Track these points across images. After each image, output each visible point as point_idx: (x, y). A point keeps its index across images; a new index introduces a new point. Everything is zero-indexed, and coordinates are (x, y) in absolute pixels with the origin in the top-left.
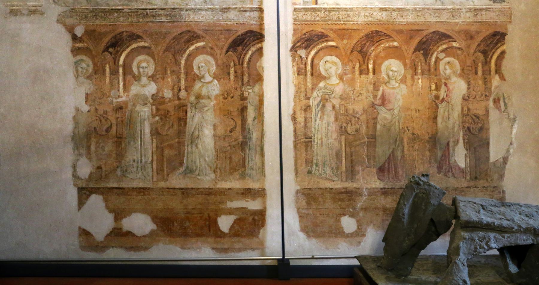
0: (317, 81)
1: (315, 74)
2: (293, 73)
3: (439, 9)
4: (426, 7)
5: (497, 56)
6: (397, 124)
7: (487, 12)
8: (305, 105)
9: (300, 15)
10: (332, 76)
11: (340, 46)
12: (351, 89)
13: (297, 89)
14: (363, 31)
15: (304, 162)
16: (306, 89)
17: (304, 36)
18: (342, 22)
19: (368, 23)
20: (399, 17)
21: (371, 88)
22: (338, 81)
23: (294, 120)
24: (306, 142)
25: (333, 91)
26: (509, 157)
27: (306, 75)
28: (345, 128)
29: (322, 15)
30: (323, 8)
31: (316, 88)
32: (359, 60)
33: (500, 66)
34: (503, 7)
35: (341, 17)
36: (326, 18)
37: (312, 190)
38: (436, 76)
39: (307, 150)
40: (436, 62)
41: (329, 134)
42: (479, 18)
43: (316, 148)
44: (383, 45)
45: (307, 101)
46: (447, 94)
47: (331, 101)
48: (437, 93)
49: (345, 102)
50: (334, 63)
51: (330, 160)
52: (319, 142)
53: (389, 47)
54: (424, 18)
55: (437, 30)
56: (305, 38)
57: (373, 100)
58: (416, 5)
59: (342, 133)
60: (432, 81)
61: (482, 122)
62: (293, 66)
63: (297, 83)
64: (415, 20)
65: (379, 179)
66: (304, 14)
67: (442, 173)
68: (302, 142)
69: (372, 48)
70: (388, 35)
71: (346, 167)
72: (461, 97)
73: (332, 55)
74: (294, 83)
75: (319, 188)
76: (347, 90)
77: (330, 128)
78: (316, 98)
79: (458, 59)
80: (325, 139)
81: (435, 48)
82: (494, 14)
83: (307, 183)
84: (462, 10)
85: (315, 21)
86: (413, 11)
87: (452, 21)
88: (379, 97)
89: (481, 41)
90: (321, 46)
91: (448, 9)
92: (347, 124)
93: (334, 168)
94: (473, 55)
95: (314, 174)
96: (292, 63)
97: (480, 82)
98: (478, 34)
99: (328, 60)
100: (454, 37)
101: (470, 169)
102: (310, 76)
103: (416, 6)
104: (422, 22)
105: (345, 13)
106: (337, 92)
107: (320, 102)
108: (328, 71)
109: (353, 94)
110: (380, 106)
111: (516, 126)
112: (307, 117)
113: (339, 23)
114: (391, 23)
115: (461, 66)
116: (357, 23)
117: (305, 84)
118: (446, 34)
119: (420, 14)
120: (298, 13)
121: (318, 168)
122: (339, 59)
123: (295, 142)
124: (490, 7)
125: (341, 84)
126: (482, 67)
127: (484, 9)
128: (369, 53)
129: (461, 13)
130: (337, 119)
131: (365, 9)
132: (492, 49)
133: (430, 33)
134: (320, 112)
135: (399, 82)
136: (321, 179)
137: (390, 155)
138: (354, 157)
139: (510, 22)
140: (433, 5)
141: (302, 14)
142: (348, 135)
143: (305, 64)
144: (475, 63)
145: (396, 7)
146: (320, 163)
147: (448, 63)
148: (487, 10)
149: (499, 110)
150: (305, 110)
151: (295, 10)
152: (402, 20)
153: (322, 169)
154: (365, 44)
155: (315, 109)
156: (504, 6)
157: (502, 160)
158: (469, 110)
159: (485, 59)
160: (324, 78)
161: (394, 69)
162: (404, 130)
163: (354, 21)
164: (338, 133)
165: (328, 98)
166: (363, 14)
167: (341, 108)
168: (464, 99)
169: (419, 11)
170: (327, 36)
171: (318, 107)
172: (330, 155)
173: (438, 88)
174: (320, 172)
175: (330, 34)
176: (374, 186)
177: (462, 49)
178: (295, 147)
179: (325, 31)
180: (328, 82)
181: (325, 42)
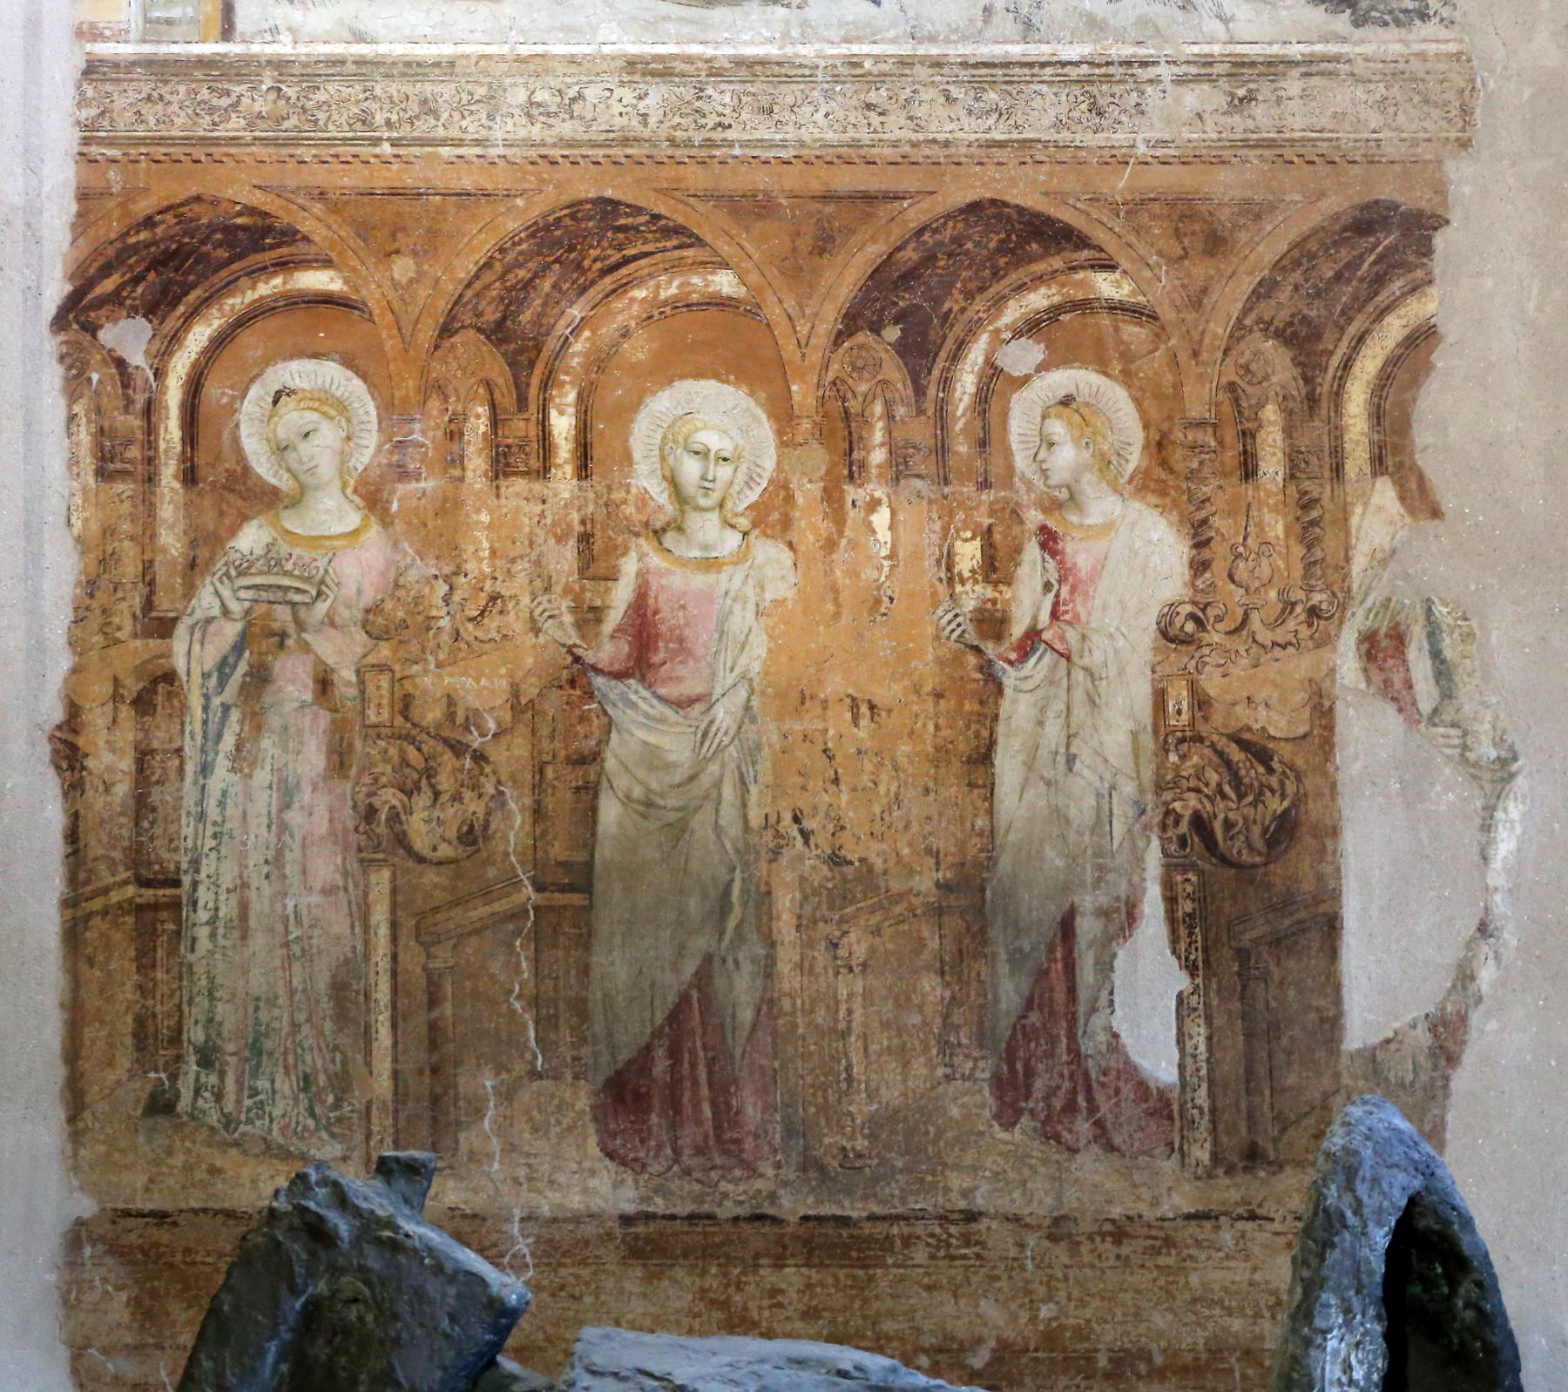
0: (221, 513)
1: (209, 476)
2: (69, 468)
3: (1006, 65)
4: (921, 51)
5: (1379, 362)
6: (728, 792)
7: (1315, 81)
8: (138, 671)
9: (120, 102)
10: (317, 488)
11: (372, 294)
12: (434, 571)
13: (93, 568)
14: (519, 202)
15: (129, 1040)
16: (148, 566)
17: (143, 236)
18: (386, 148)
19: (551, 152)
20: (745, 116)
21: (564, 560)
22: (353, 519)
23: (72, 768)
24: (140, 909)
25: (322, 582)
26: (1475, 1018)
27: (151, 479)
28: (394, 817)
29: (261, 106)
30: (269, 62)
31: (211, 560)
32: (489, 385)
33: (1403, 426)
34: (1416, 48)
35: (379, 118)
36: (286, 124)
37: (175, 1224)
38: (985, 485)
39: (145, 962)
40: (983, 398)
41: (288, 856)
42: (1262, 118)
43: (204, 944)
44: (640, 293)
45: (154, 643)
46: (1056, 604)
47: (306, 647)
48: (990, 593)
49: (395, 651)
50: (337, 407)
51: (295, 1026)
52: (228, 909)
53: (683, 305)
54: (911, 118)
55: (988, 195)
56: (147, 245)
57: (575, 640)
58: (859, 40)
59: (377, 848)
60: (961, 516)
61: (1291, 787)
62: (72, 418)
63: (95, 527)
64: (851, 133)
65: (610, 1155)
66: (149, 99)
67: (1025, 1120)
68: (119, 905)
69: (576, 312)
70: (679, 230)
71: (396, 1075)
72: (1150, 620)
73: (316, 355)
74: (76, 531)
75: (217, 1212)
76: (412, 576)
77: (294, 817)
78: (212, 628)
79: (1127, 378)
80: (267, 889)
81: (979, 304)
82: (1360, 92)
83: (140, 1180)
84: (1151, 72)
85: (215, 142)
86: (836, 78)
87: (1090, 139)
88: (613, 618)
89: (1277, 265)
90: (250, 296)
91: (1064, 64)
92: (410, 794)
93: (322, 1080)
94: (1226, 352)
95: (192, 1117)
96: (62, 402)
97: (1276, 527)
98: (1258, 217)
99: (291, 384)
100: (1100, 236)
101: (1211, 1095)
102: (177, 485)
103: (855, 49)
104: (895, 144)
105: (407, 88)
106: (350, 589)
107: (238, 648)
108: (291, 457)
109: (447, 600)
110: (619, 676)
111: (1513, 811)
112: (155, 745)
113: (366, 151)
114: (693, 152)
115: (1146, 426)
116: (478, 151)
117: (147, 536)
118: (1050, 222)
119: (883, 92)
120: (108, 87)
121: (213, 1079)
122: (364, 376)
123: (68, 904)
124: (1333, 48)
125: (375, 530)
126: (1288, 431)
127: (1291, 63)
128: (552, 344)
129: (1149, 90)
130: (342, 763)
131: (534, 65)
132: (1347, 315)
133: (948, 217)
134: (235, 715)
135: (744, 523)
136: (234, 1151)
137: (684, 1000)
138: (448, 1009)
139: (1464, 144)
140: (964, 38)
141: (133, 96)
142: (410, 864)
143: (150, 411)
144: (1236, 401)
145: (729, 51)
146: (230, 1047)
147: (1066, 401)
148: (1314, 69)
149: (1400, 710)
150: (143, 704)
151: (93, 70)
152: (764, 133)
153: (239, 1082)
154: (528, 285)
155: (206, 697)
156: (1424, 46)
157: (1423, 1037)
158: (1201, 703)
159: (1307, 380)
160: (267, 499)
161: (712, 440)
162: (778, 835)
163: (460, 143)
164: (346, 850)
165: (291, 629)
166: (521, 96)
167: (370, 688)
168: (1168, 634)
169: (875, 80)
170: (290, 235)
171: (222, 684)
172: (292, 993)
173: (995, 567)
174: (229, 1107)
175: (306, 226)
176: (575, 1202)
177: (1154, 317)
178: (73, 936)
179: (279, 202)
180: (291, 521)
181: (275, 274)
